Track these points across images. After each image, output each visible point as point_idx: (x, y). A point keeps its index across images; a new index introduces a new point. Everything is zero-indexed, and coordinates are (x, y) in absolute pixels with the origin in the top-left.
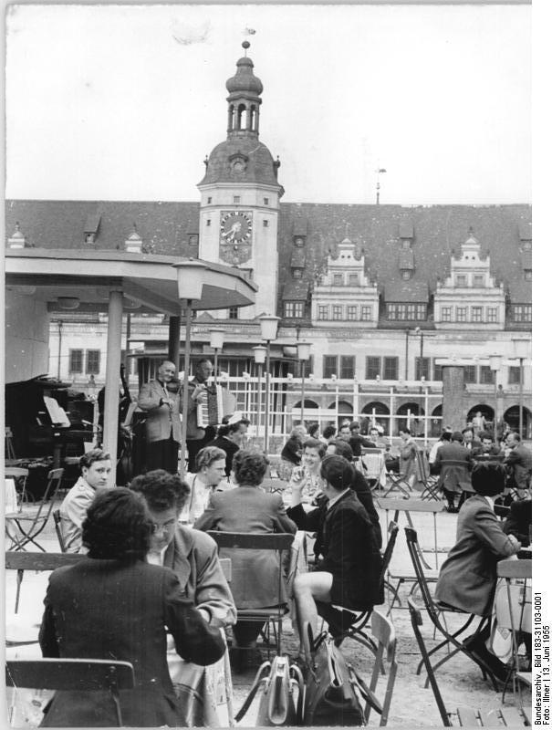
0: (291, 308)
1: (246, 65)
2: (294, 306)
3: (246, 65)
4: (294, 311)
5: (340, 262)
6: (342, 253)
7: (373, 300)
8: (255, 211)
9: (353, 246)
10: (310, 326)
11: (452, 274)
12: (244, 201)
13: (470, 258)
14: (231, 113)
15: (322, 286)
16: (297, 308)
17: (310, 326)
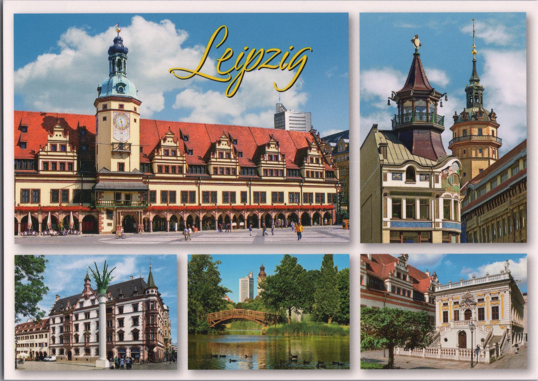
8: (131, 113)
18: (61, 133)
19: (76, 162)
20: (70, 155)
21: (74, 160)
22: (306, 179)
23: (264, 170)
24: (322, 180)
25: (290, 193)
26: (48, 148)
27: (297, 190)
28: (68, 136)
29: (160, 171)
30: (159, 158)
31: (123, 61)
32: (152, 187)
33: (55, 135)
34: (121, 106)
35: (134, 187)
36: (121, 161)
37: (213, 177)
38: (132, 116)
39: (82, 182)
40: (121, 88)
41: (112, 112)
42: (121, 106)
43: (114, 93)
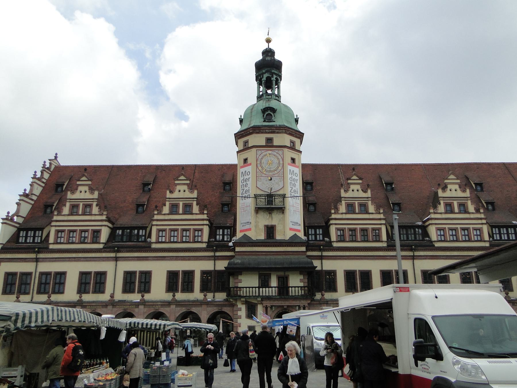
0: (313, 233)
1: (268, 53)
2: (315, 232)
3: (268, 53)
4: (316, 234)
5: (350, 194)
6: (352, 187)
7: (381, 224)
8: (286, 150)
9: (360, 181)
10: (329, 246)
11: (442, 202)
12: (275, 144)
13: (453, 190)
15: (338, 214)
16: (318, 233)
17: (329, 246)
18: (185, 187)
20: (199, 220)
26: (166, 209)
28: (196, 192)
29: (341, 238)
31: (274, 79)
32: (328, 265)
33: (177, 191)
34: (269, 140)
36: (269, 223)
38: (289, 154)
39: (215, 258)
40: (269, 115)
41: (254, 150)
43: (258, 121)
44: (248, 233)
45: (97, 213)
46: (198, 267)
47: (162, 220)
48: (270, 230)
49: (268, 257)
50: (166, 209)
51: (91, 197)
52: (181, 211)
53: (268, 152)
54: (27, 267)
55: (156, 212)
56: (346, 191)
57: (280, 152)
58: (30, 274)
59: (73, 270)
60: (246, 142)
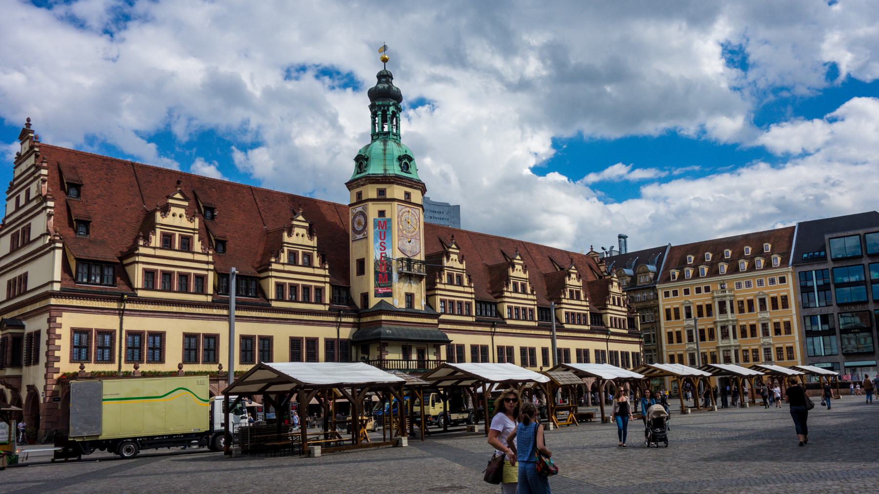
14: (374, 115)
18: (304, 231)
19: (327, 286)
21: (325, 282)
22: (612, 330)
23: (567, 313)
24: (626, 332)
25: (597, 352)
27: (602, 346)
28: (316, 238)
30: (442, 287)
33: (295, 234)
35: (432, 336)
37: (509, 322)
39: (339, 325)
42: (408, 195)
43: (395, 169)
44: (388, 300)
45: (200, 251)
46: (323, 333)
47: (281, 272)
48: (410, 297)
49: (410, 328)
50: (284, 257)
51: (191, 225)
52: (300, 263)
53: (406, 208)
54: (109, 322)
55: (273, 260)
56: (448, 259)
57: (417, 211)
58: (111, 333)
59: (174, 330)
60: (382, 192)
